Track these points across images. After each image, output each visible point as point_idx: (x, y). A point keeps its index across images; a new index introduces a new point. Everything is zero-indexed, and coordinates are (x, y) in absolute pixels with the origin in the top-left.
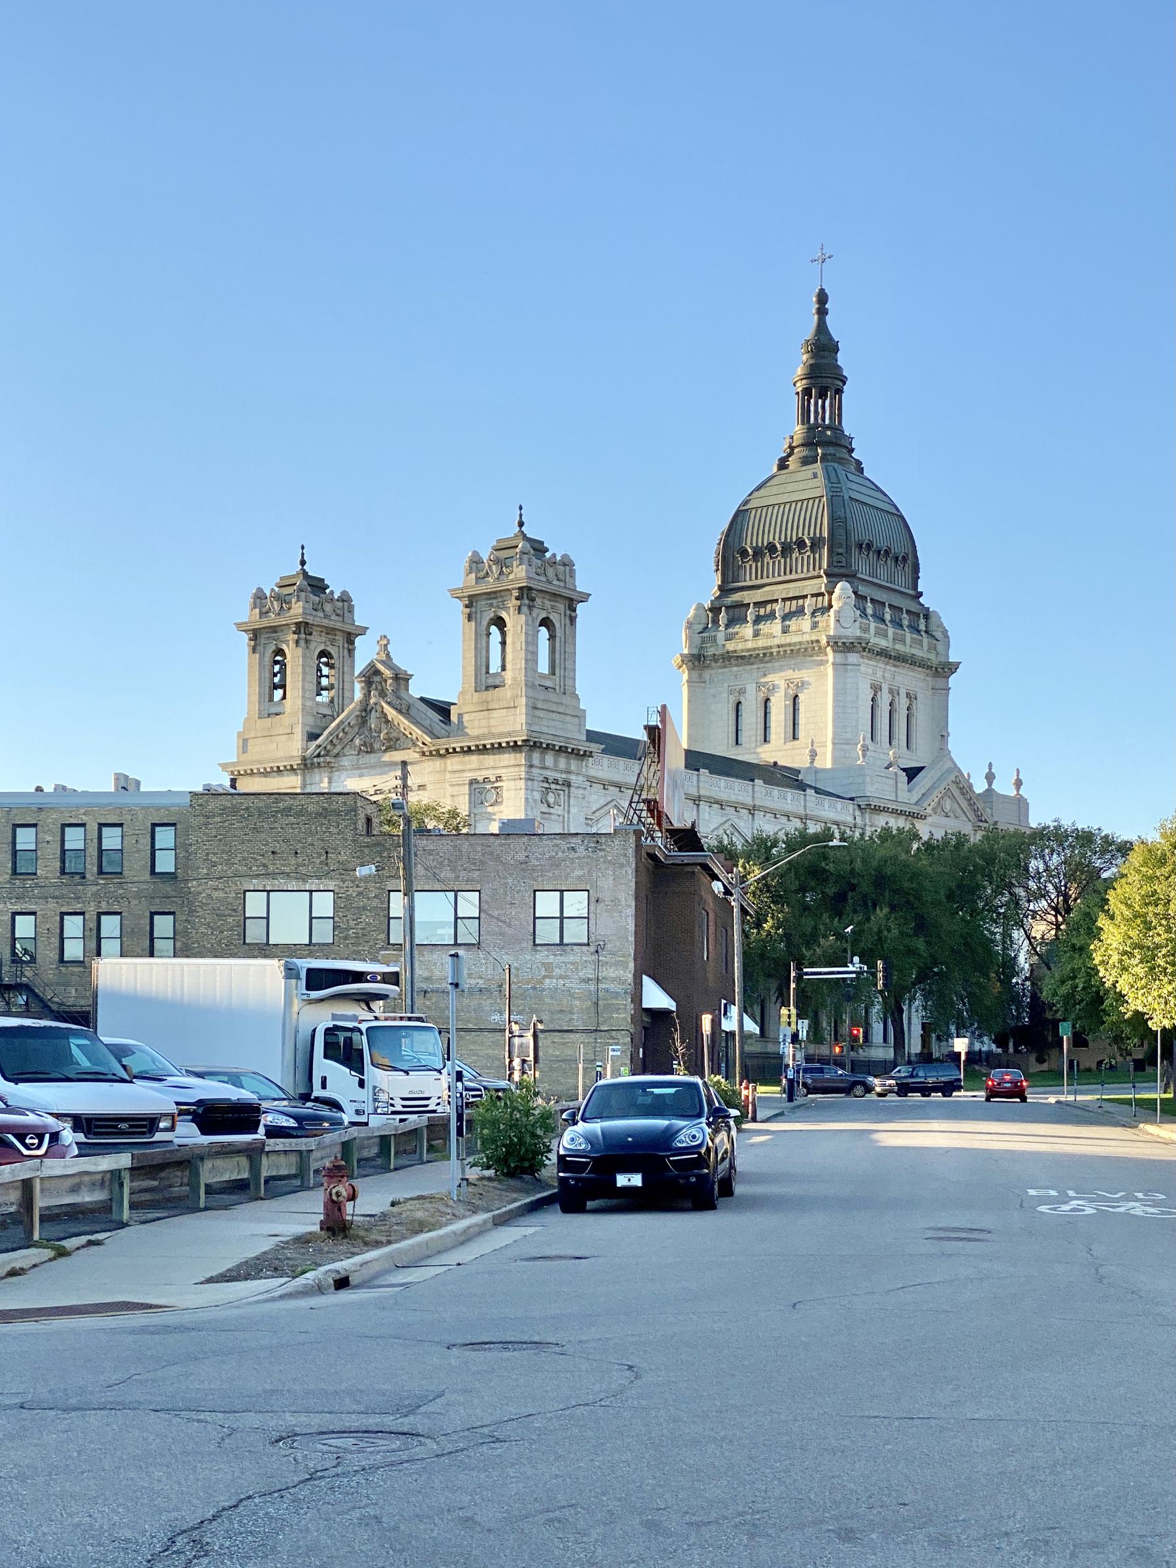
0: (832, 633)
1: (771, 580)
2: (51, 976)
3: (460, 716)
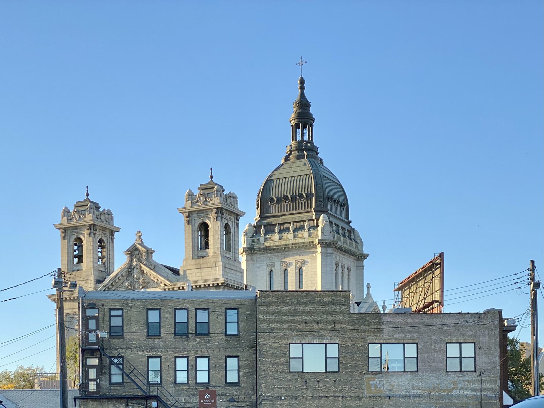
2: (170, 392)
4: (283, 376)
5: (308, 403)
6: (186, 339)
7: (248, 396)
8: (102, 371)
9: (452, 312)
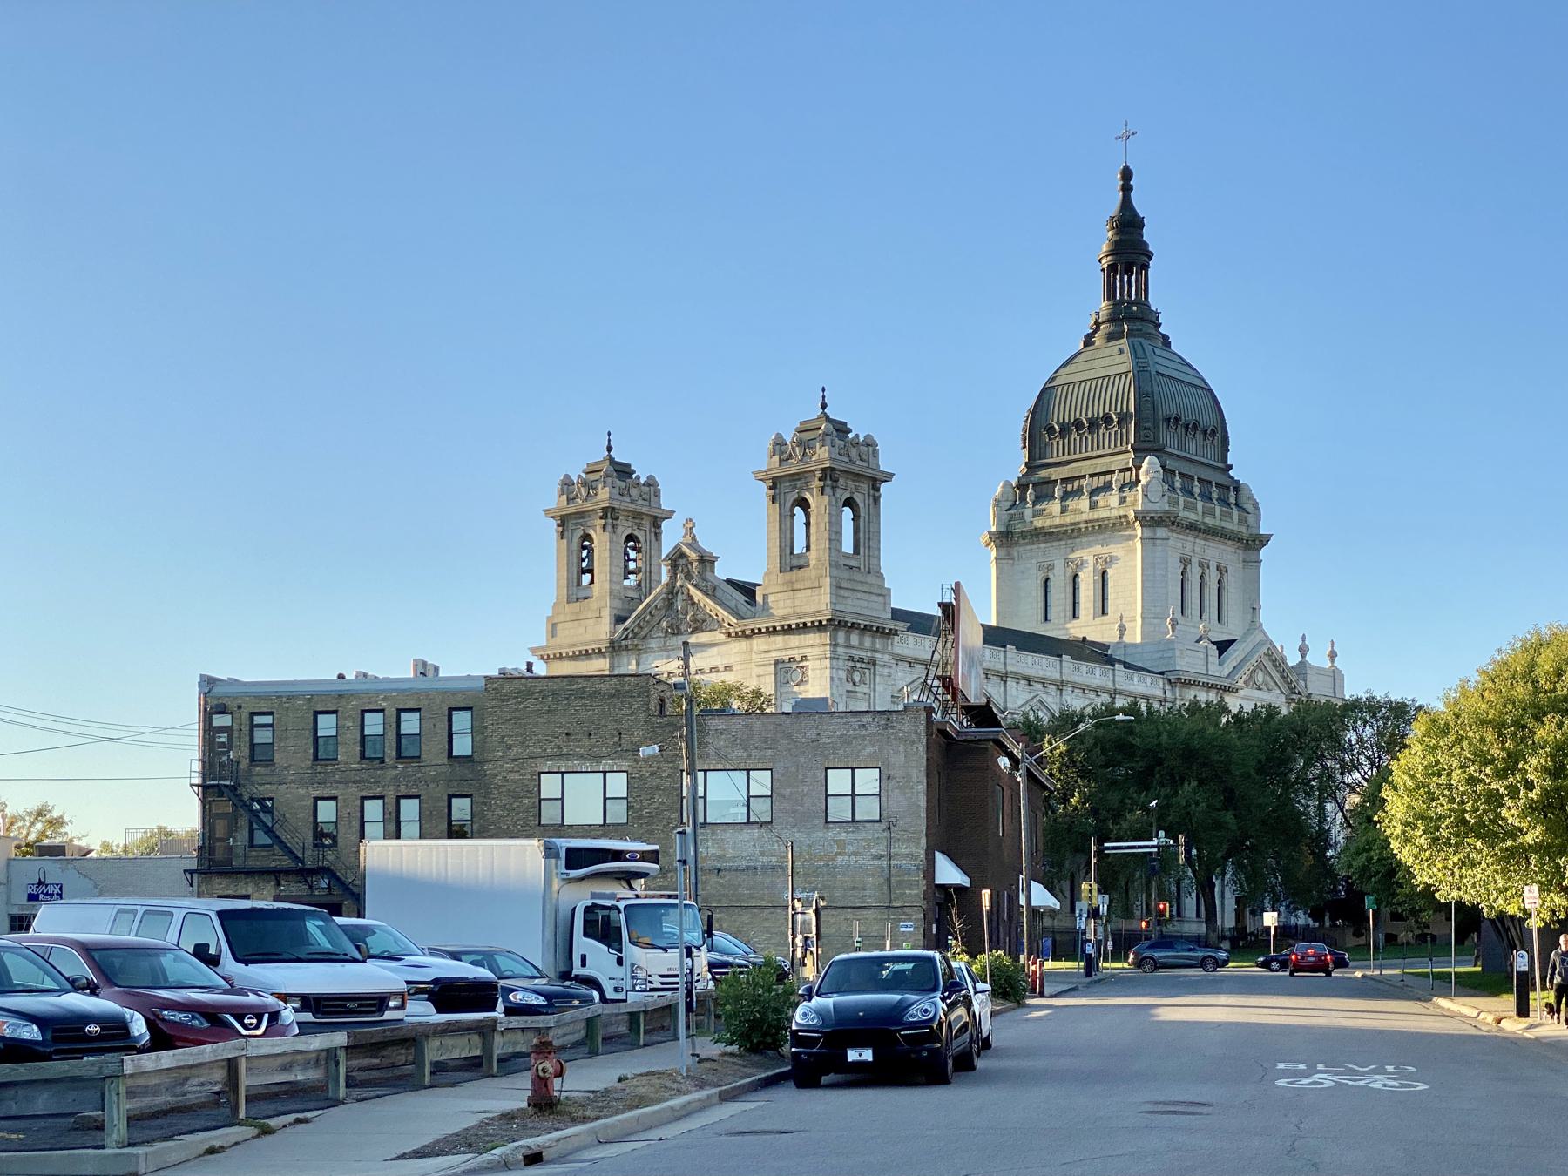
0: (1140, 508)
1: (1078, 456)
3: (765, 597)
8: (237, 823)
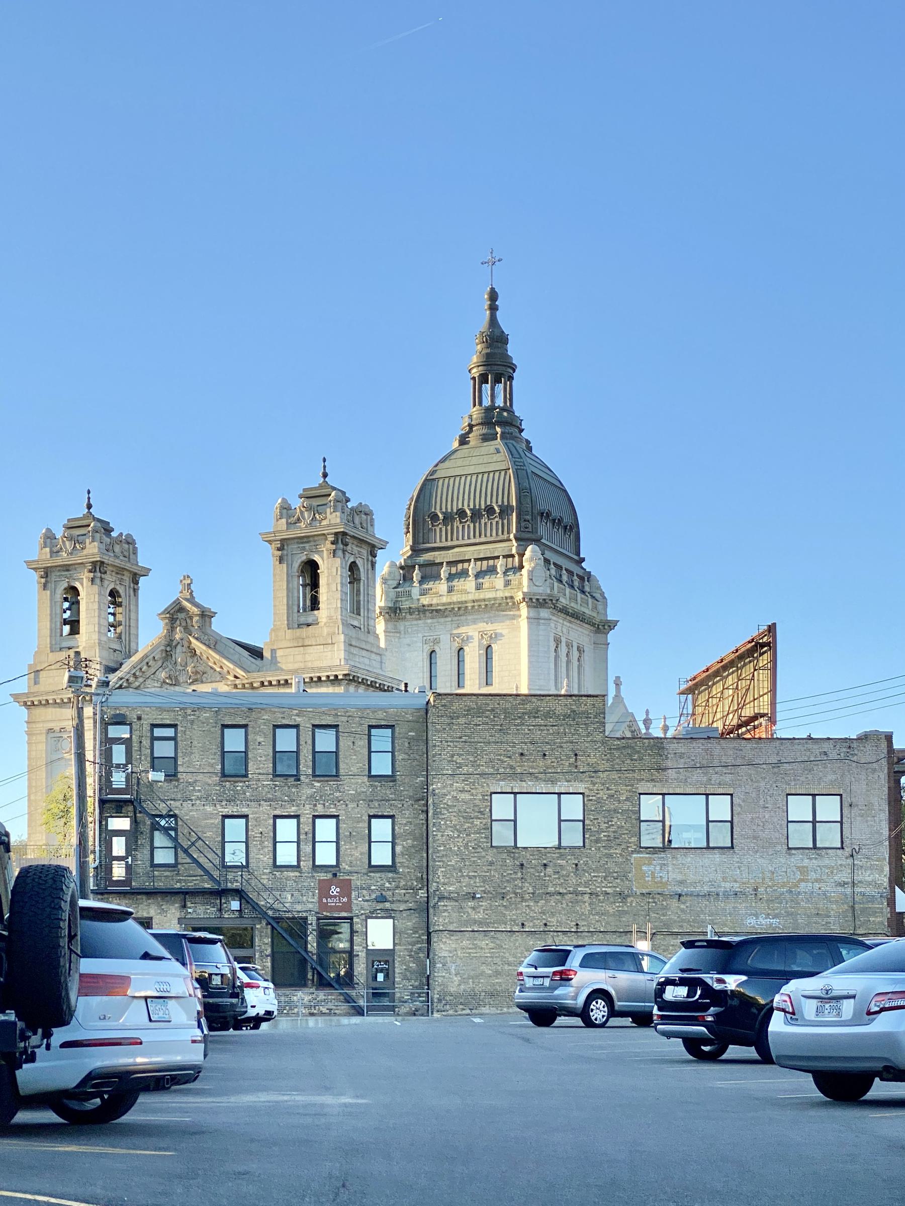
2: (265, 882)
4: (479, 854)
5: (526, 906)
6: (296, 783)
7: (412, 891)
8: (137, 842)
9: (797, 737)
